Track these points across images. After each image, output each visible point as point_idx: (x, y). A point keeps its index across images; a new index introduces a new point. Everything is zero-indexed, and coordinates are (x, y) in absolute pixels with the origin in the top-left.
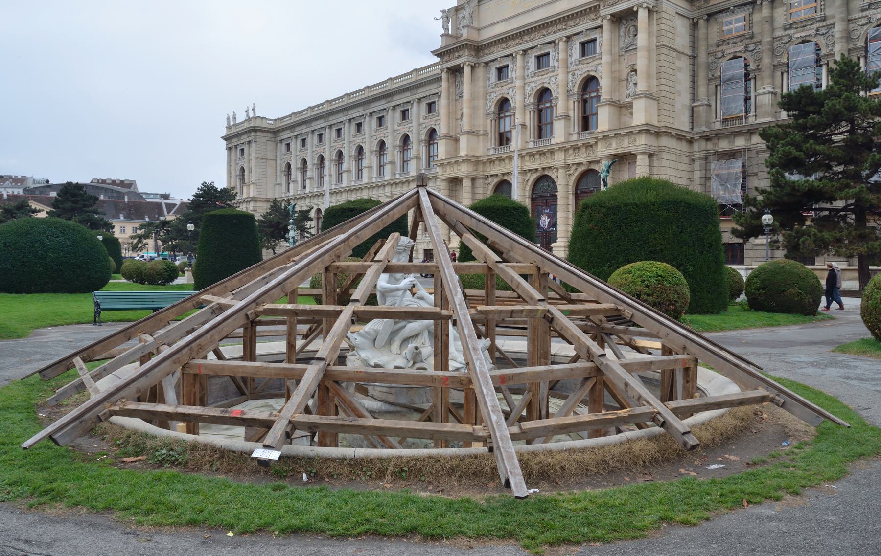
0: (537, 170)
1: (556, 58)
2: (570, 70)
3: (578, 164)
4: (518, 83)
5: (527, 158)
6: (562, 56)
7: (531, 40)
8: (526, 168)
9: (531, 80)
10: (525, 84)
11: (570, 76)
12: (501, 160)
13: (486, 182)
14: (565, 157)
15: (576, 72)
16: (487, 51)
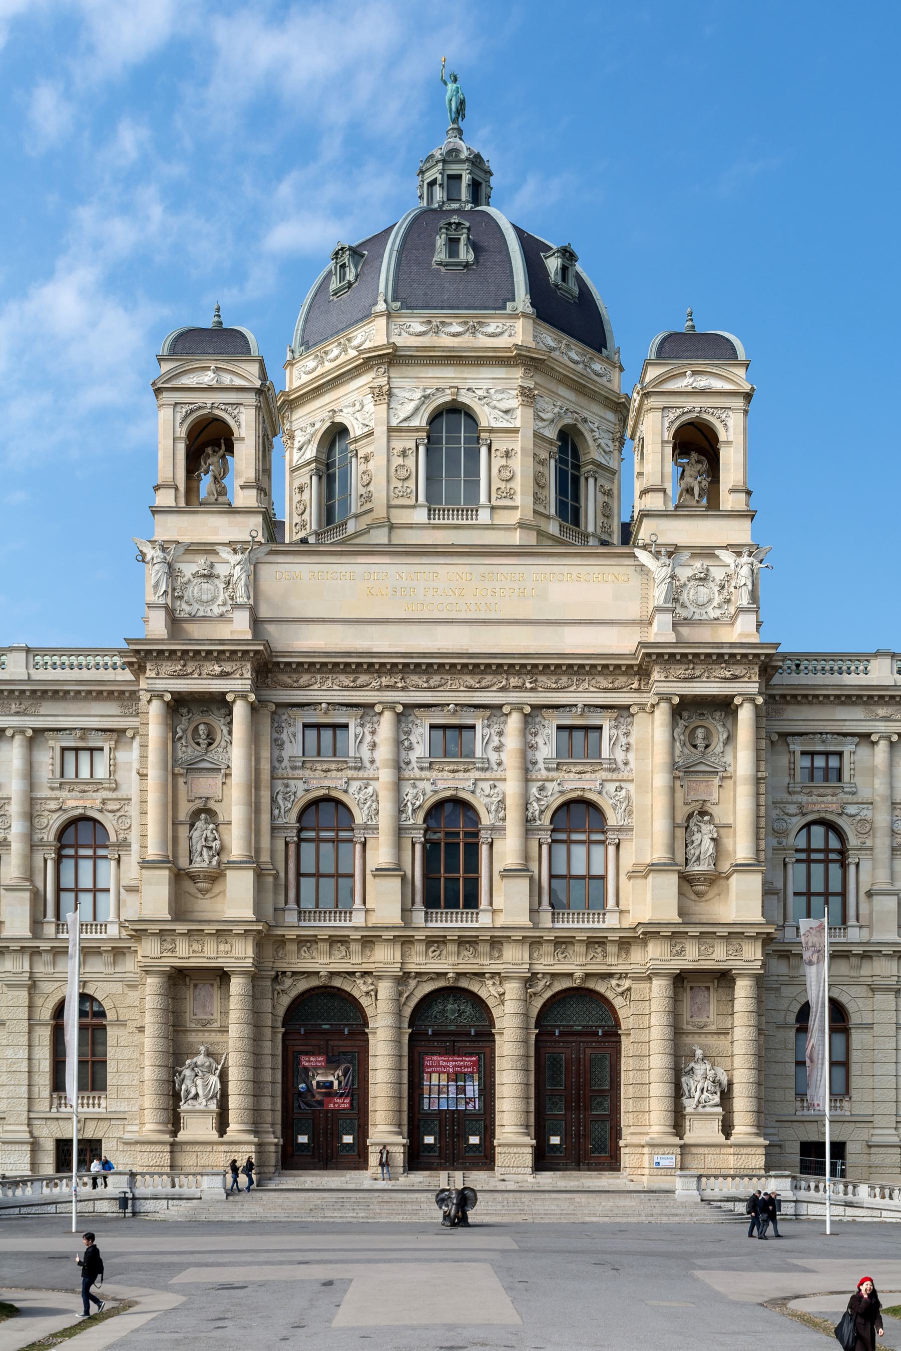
0: (442, 975)
1: (492, 745)
2: (534, 775)
3: (554, 976)
4: (386, 775)
5: (420, 947)
6: (512, 741)
7: (430, 689)
8: (412, 968)
9: (417, 773)
10: (400, 779)
11: (534, 791)
12: (338, 941)
13: (278, 987)
14: (531, 957)
15: (550, 786)
16: (286, 679)
